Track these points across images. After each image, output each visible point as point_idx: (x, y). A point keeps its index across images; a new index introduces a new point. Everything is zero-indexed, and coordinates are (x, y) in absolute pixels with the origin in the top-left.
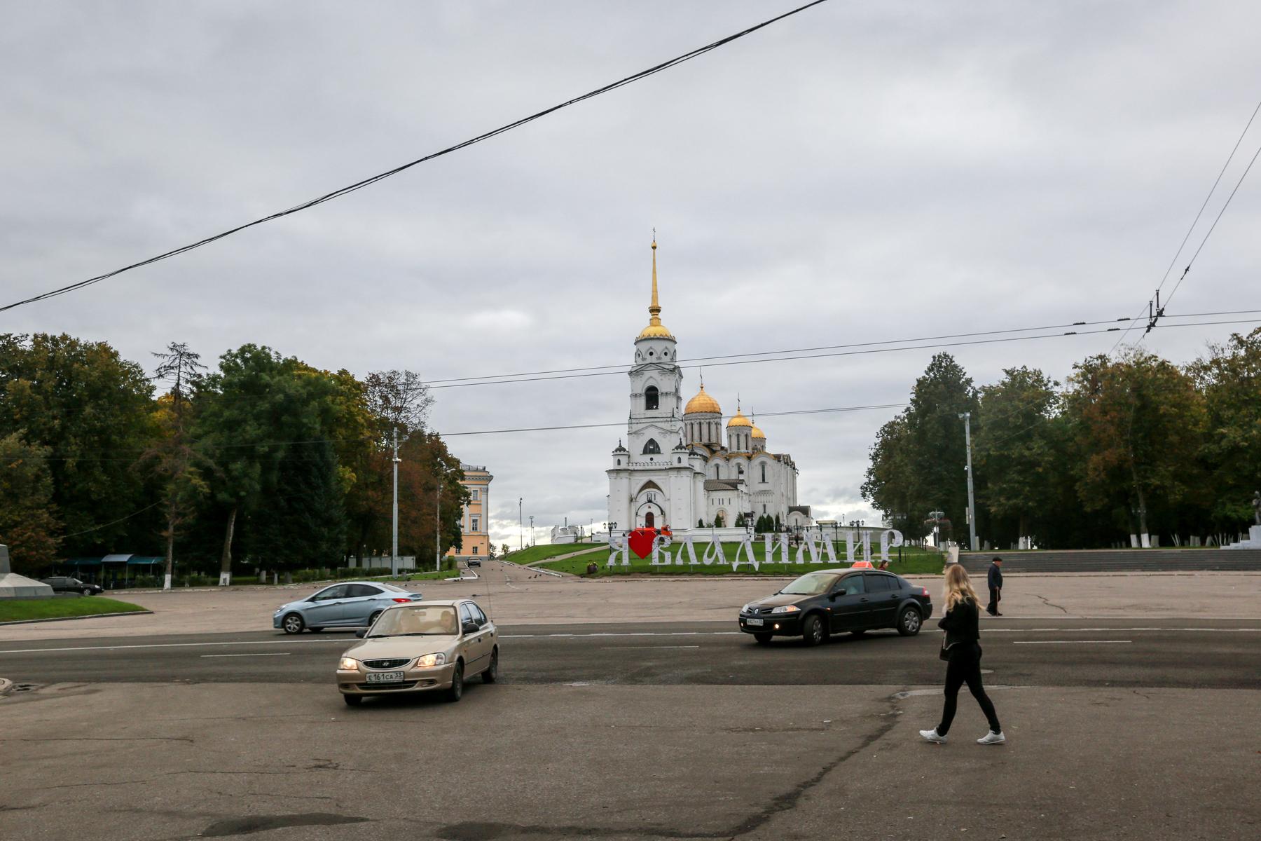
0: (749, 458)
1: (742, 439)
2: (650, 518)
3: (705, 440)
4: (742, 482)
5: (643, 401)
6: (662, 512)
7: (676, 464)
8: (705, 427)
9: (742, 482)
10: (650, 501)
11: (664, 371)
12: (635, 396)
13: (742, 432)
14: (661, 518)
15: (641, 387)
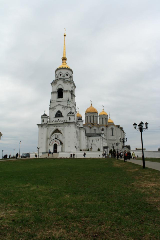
0: (107, 126)
1: (104, 120)
2: (55, 146)
3: (92, 122)
4: (103, 134)
5: (56, 95)
6: (61, 143)
7: (68, 121)
8: (92, 118)
9: (103, 134)
10: (56, 138)
11: (65, 81)
12: (53, 93)
13: (105, 117)
14: (61, 146)
15: (56, 88)
